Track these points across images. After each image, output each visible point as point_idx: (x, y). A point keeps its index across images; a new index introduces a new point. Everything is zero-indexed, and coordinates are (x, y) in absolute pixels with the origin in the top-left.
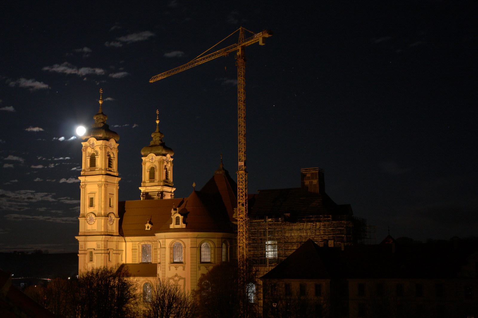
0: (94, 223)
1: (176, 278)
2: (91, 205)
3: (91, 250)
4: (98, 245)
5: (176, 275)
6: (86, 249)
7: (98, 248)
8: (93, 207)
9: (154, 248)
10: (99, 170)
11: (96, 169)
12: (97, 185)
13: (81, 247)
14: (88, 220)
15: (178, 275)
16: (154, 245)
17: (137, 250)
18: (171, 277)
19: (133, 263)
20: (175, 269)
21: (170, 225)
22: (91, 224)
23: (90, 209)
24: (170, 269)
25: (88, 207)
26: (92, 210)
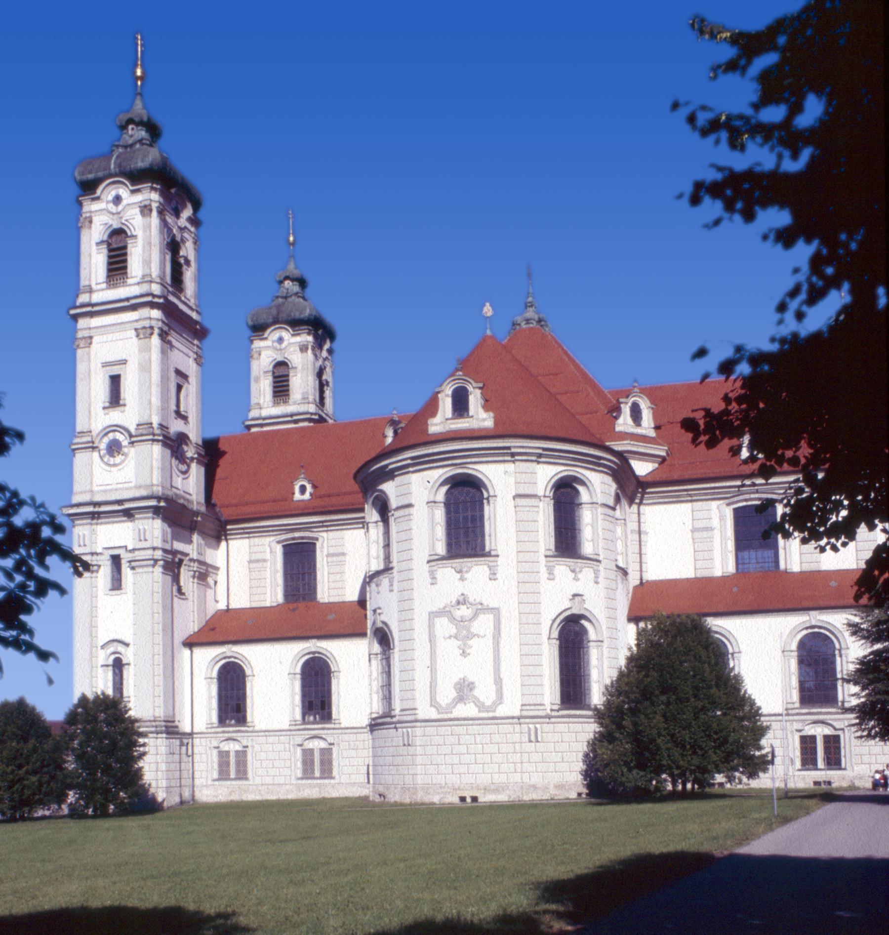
0: (123, 462)
1: (464, 611)
2: (115, 399)
3: (115, 552)
4: (142, 531)
5: (462, 601)
6: (99, 550)
7: (140, 540)
8: (122, 408)
9: (325, 553)
10: (138, 283)
11: (130, 281)
12: (133, 333)
13: (82, 543)
14: (102, 452)
15: (471, 600)
16: (326, 542)
17: (269, 563)
18: (441, 607)
19: (255, 605)
20: (458, 576)
21: (431, 421)
22: (115, 465)
23: (107, 414)
24: (434, 578)
25: (104, 408)
26: (116, 417)
